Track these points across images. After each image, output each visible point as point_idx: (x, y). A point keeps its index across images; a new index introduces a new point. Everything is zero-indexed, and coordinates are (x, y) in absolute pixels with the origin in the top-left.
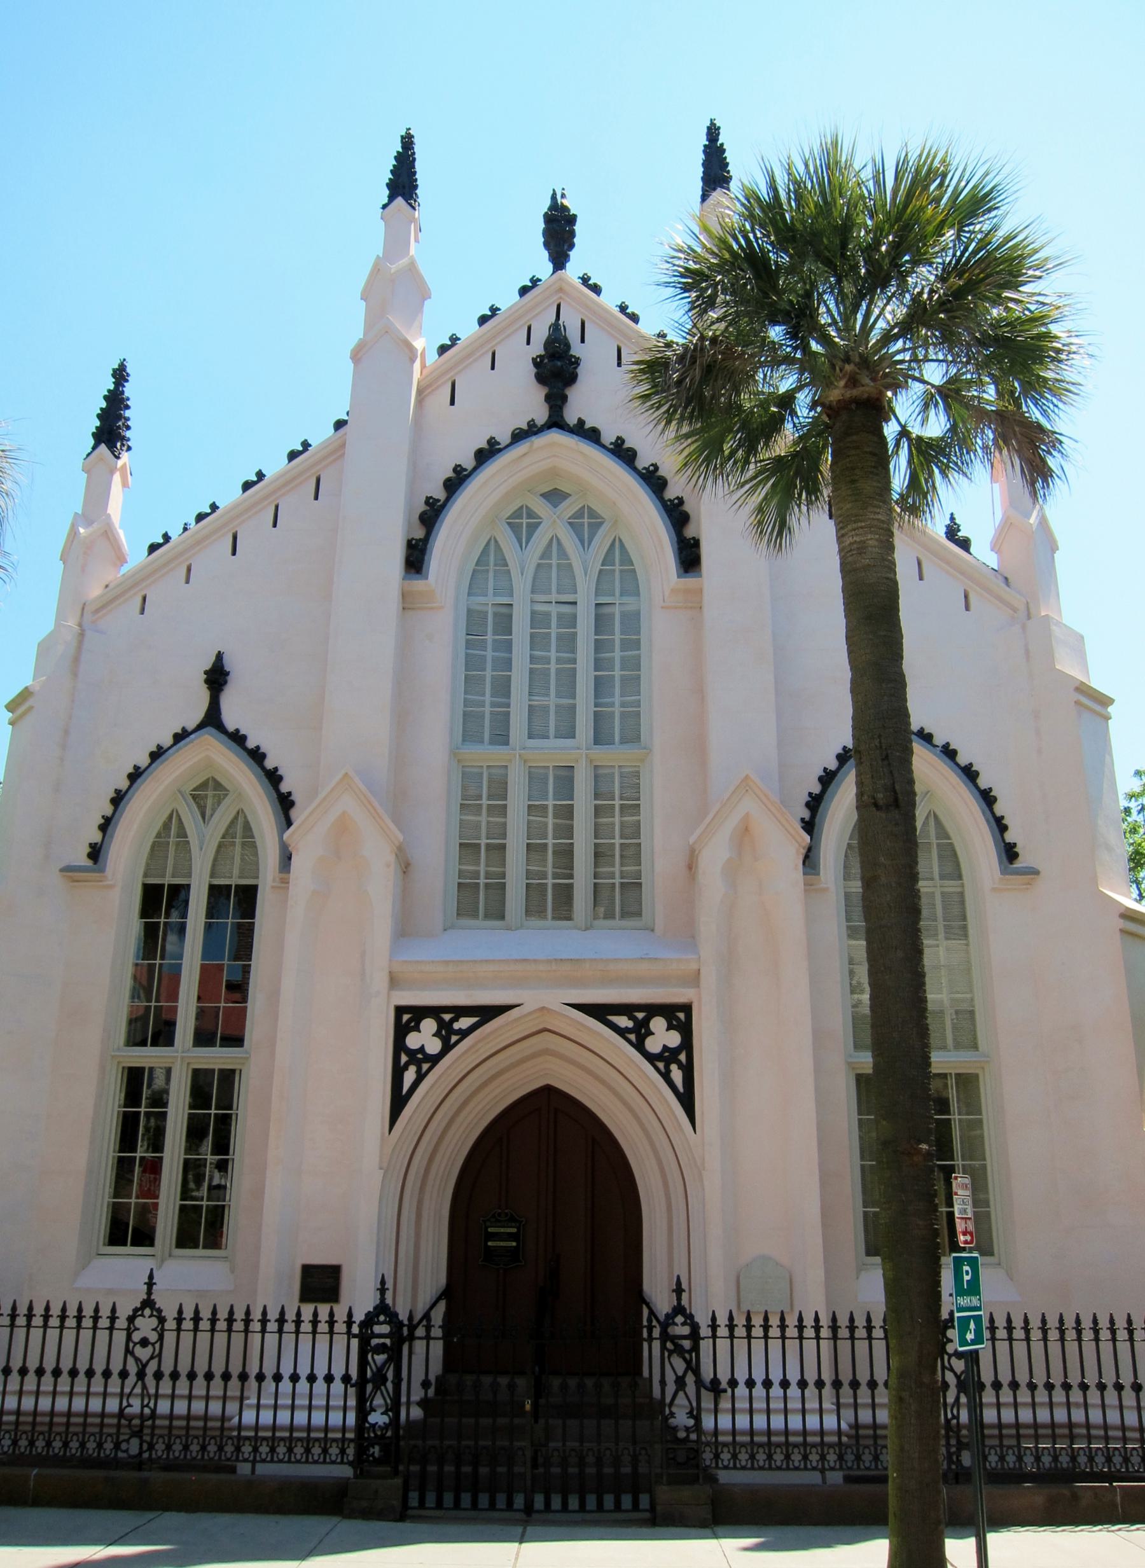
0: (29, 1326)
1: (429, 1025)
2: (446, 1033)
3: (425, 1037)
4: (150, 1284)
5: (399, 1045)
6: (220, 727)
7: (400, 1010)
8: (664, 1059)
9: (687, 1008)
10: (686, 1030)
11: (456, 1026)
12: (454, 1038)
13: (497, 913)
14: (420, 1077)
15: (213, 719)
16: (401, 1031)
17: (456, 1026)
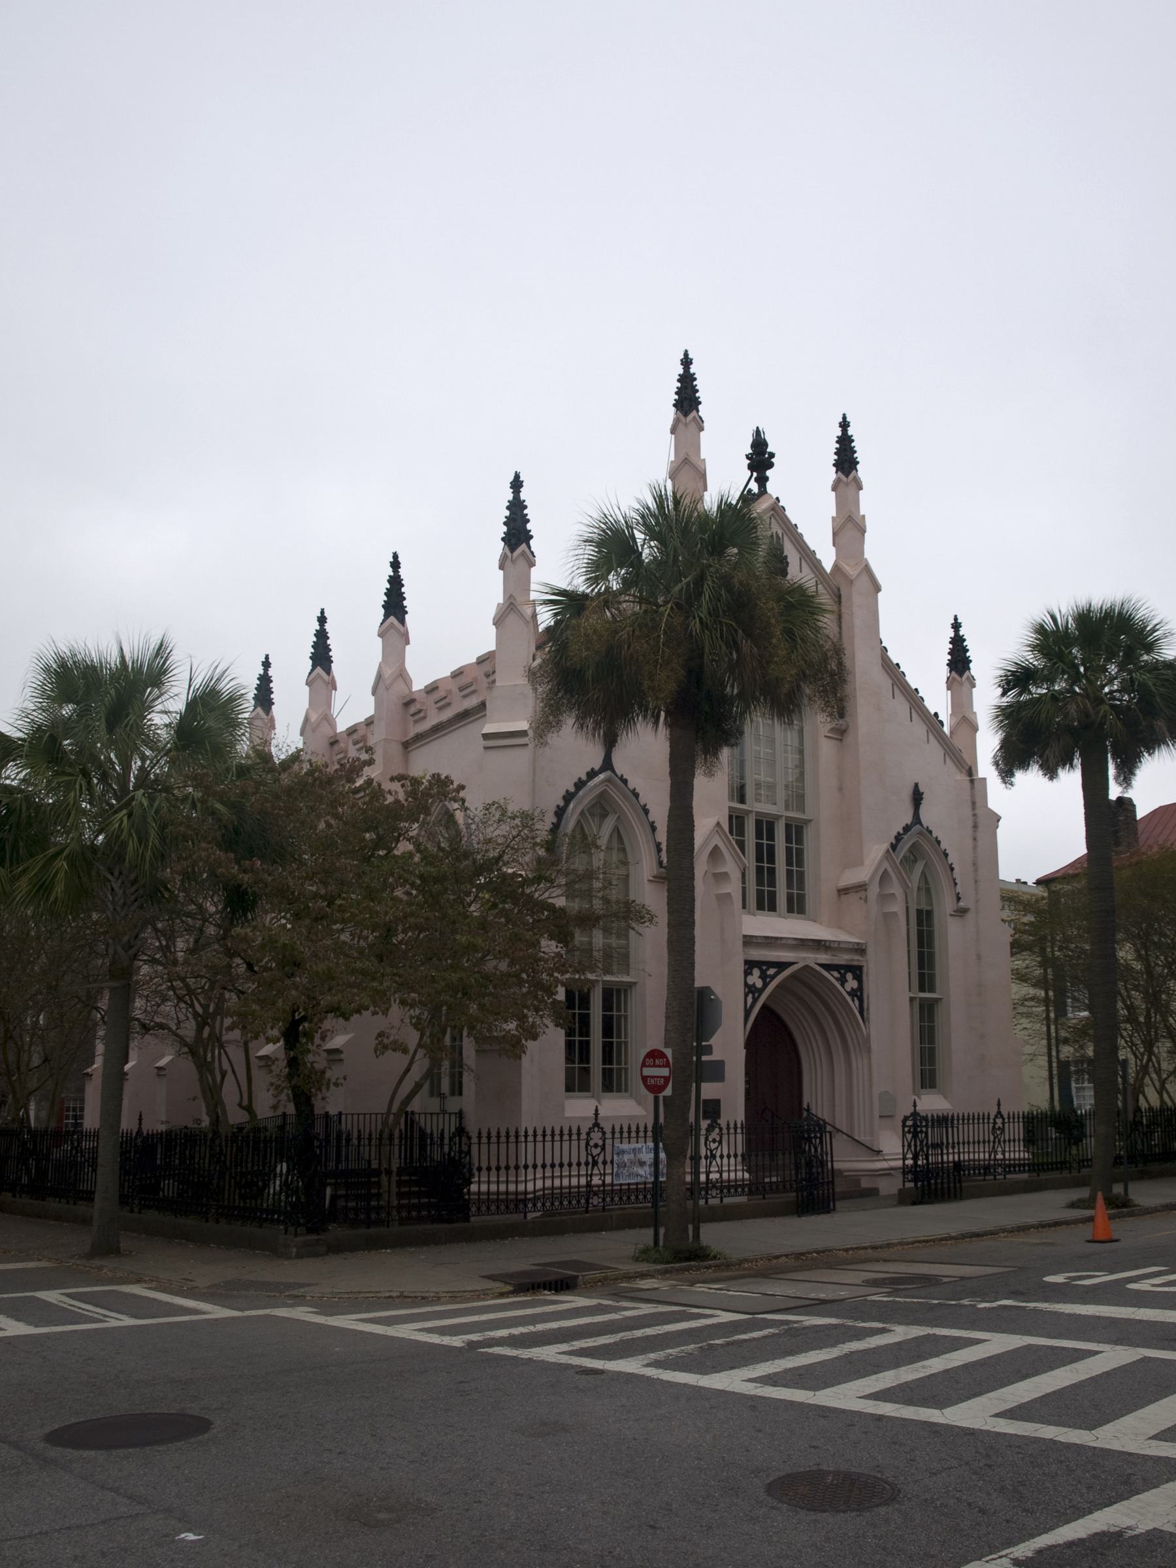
0: (561, 1140)
1: (756, 972)
2: (763, 976)
3: (755, 979)
4: (596, 1114)
5: (746, 984)
6: (614, 772)
7: (747, 962)
8: (854, 993)
9: (860, 968)
10: (859, 977)
11: (768, 973)
12: (768, 980)
13: (772, 908)
14: (755, 1000)
15: (607, 765)
16: (747, 973)
17: (768, 973)
